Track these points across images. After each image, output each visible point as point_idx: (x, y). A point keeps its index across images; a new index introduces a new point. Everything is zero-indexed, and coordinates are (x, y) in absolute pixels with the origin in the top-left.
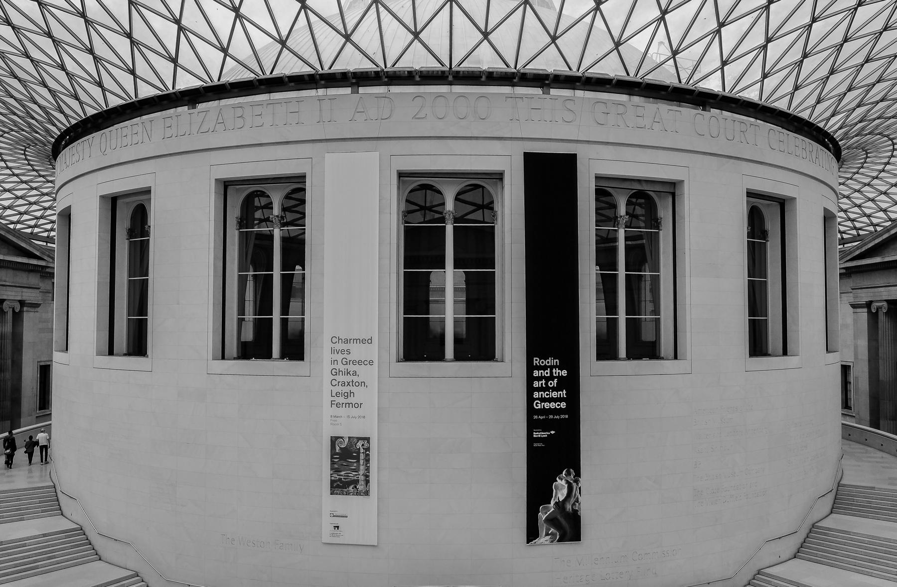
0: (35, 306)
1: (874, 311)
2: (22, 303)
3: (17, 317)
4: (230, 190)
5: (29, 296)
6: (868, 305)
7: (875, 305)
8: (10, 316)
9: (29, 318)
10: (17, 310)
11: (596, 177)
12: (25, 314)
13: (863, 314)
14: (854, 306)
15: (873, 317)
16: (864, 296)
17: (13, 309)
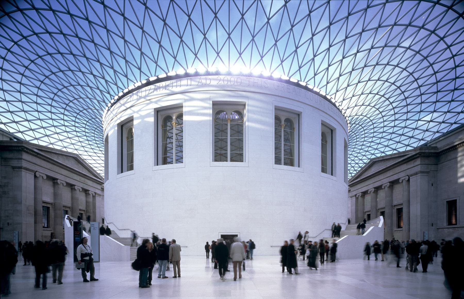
0: (100, 195)
1: (357, 197)
2: (95, 193)
3: (94, 197)
4: (159, 114)
5: (99, 192)
6: (356, 195)
7: (357, 195)
8: (92, 195)
9: (98, 198)
10: (94, 195)
11: (275, 109)
12: (96, 197)
13: (354, 199)
14: (351, 197)
15: (357, 199)
16: (354, 193)
17: (93, 194)
